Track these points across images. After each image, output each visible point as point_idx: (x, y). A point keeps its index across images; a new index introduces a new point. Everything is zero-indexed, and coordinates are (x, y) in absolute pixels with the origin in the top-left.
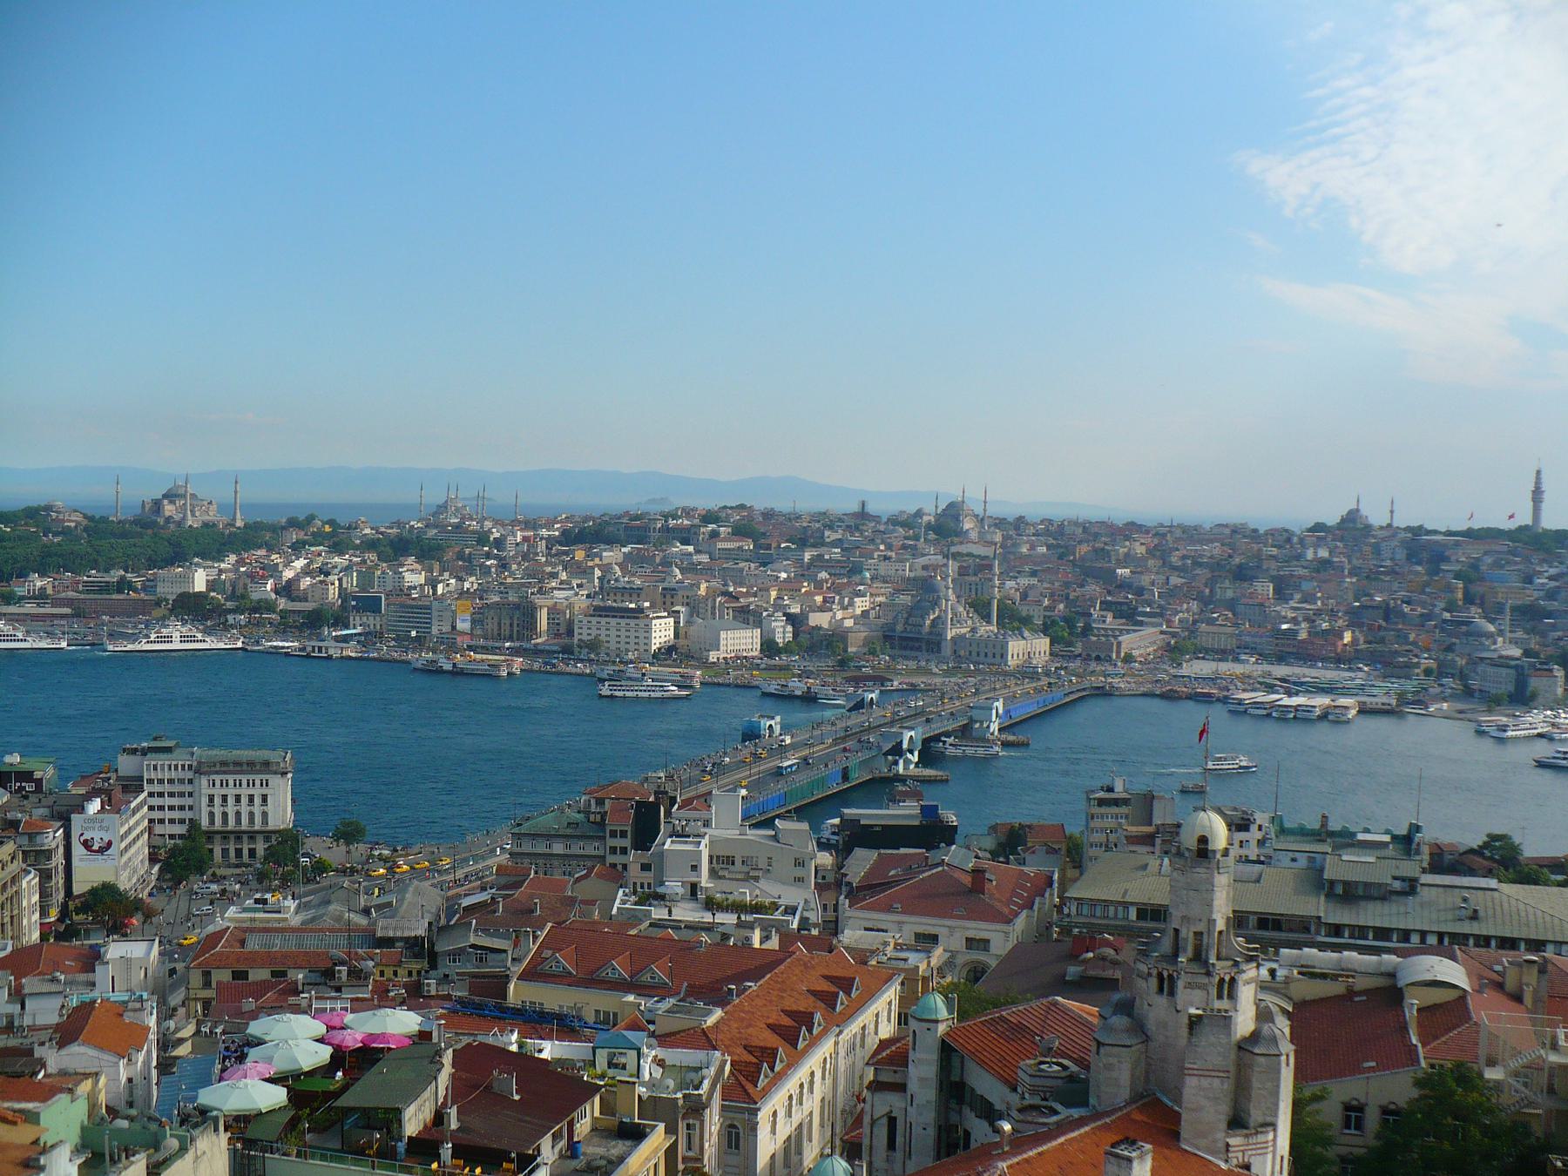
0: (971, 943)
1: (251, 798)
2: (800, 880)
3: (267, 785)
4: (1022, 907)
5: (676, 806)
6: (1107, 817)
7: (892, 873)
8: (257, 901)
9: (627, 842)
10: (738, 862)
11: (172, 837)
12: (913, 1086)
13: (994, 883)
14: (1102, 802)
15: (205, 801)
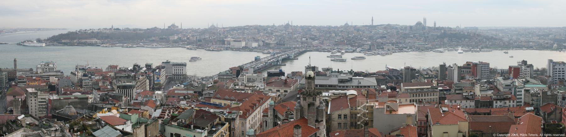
0: (285, 91)
1: (180, 70)
2: (261, 82)
4: (292, 85)
7: (273, 80)
8: (178, 85)
9: (235, 76)
10: (252, 79)
11: (169, 75)
12: (269, 116)
14: (307, 68)
15: (174, 70)
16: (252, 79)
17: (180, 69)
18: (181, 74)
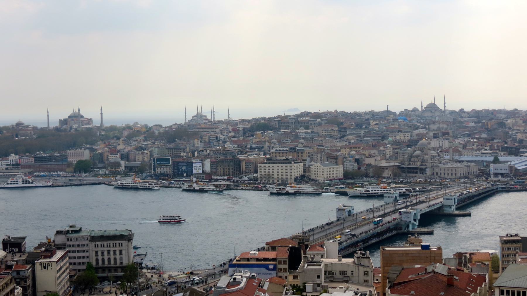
3: (122, 246)
4: (472, 292)
5: (308, 249)
6: (510, 249)
7: (410, 277)
9: (286, 266)
13: (458, 281)
15: (94, 253)
16: (338, 274)
17: (112, 249)
18: (118, 265)
